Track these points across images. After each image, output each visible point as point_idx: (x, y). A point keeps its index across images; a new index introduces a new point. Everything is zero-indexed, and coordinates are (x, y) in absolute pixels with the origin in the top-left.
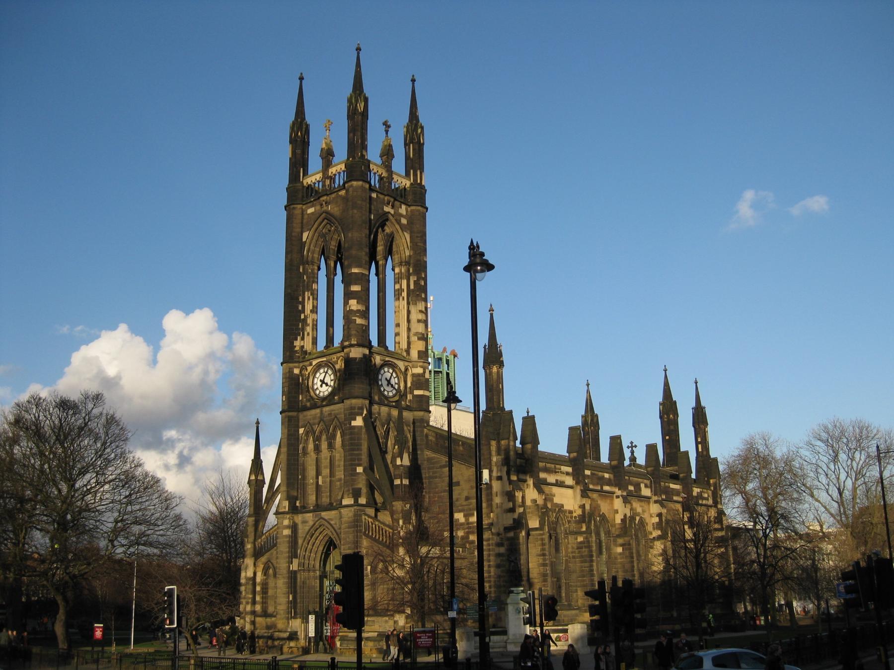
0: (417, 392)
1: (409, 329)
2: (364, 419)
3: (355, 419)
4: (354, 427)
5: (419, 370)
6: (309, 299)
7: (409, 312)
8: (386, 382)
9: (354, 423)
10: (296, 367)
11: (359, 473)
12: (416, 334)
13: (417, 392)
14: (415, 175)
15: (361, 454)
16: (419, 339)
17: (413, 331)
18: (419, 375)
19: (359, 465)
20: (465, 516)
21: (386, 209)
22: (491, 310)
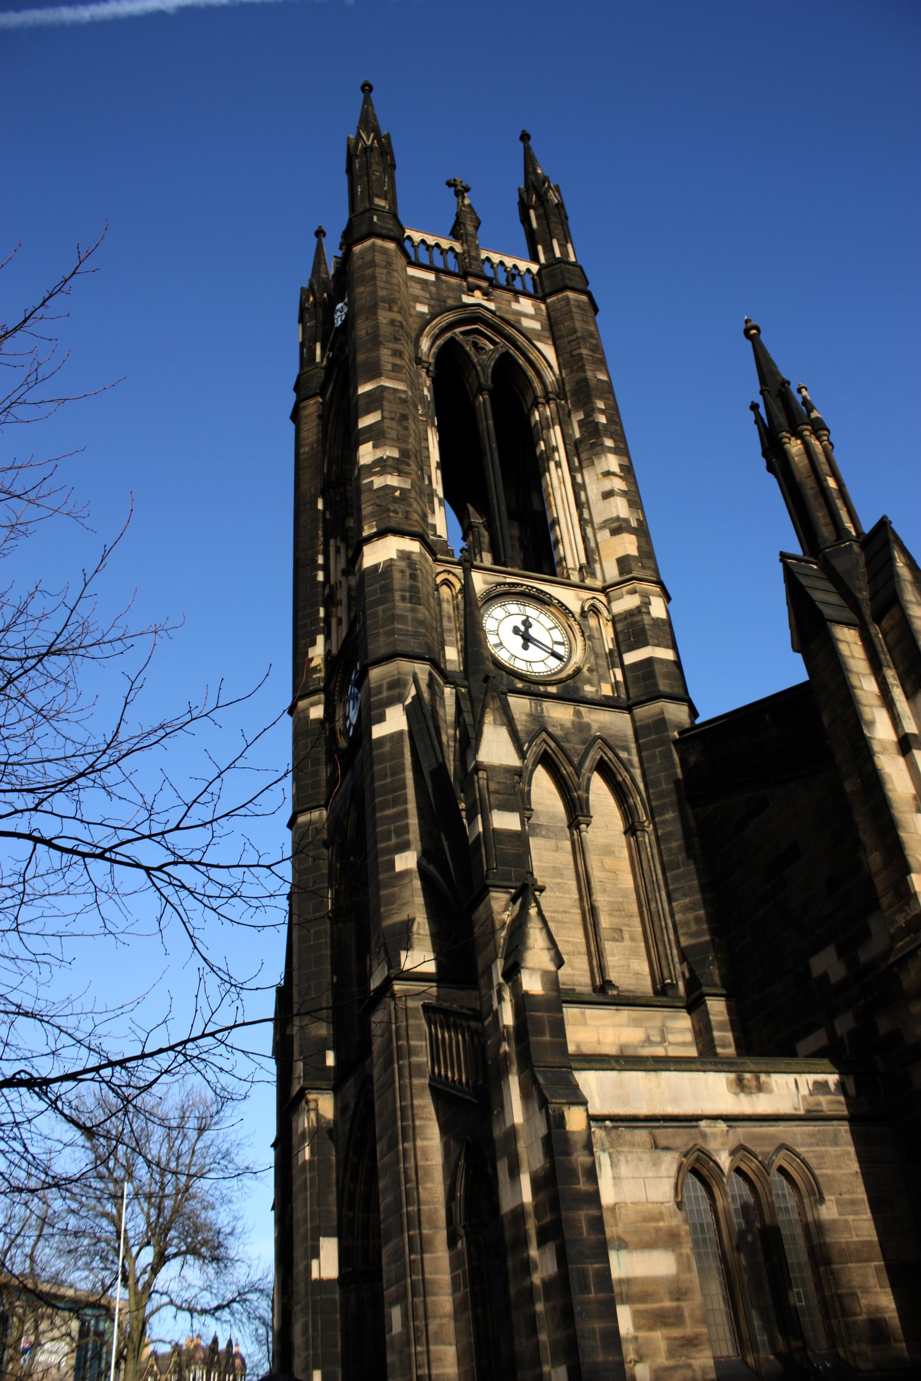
0: (630, 658)
1: (583, 523)
2: (410, 712)
3: (381, 718)
4: (382, 740)
5: (626, 603)
6: (338, 550)
7: (578, 488)
8: (519, 640)
9: (378, 731)
10: (313, 704)
11: (405, 873)
12: (605, 524)
13: (630, 658)
14: (549, 250)
15: (404, 814)
16: (615, 532)
17: (598, 520)
18: (630, 614)
19: (404, 847)
20: (841, 954)
21: (466, 299)
22: (751, 333)
